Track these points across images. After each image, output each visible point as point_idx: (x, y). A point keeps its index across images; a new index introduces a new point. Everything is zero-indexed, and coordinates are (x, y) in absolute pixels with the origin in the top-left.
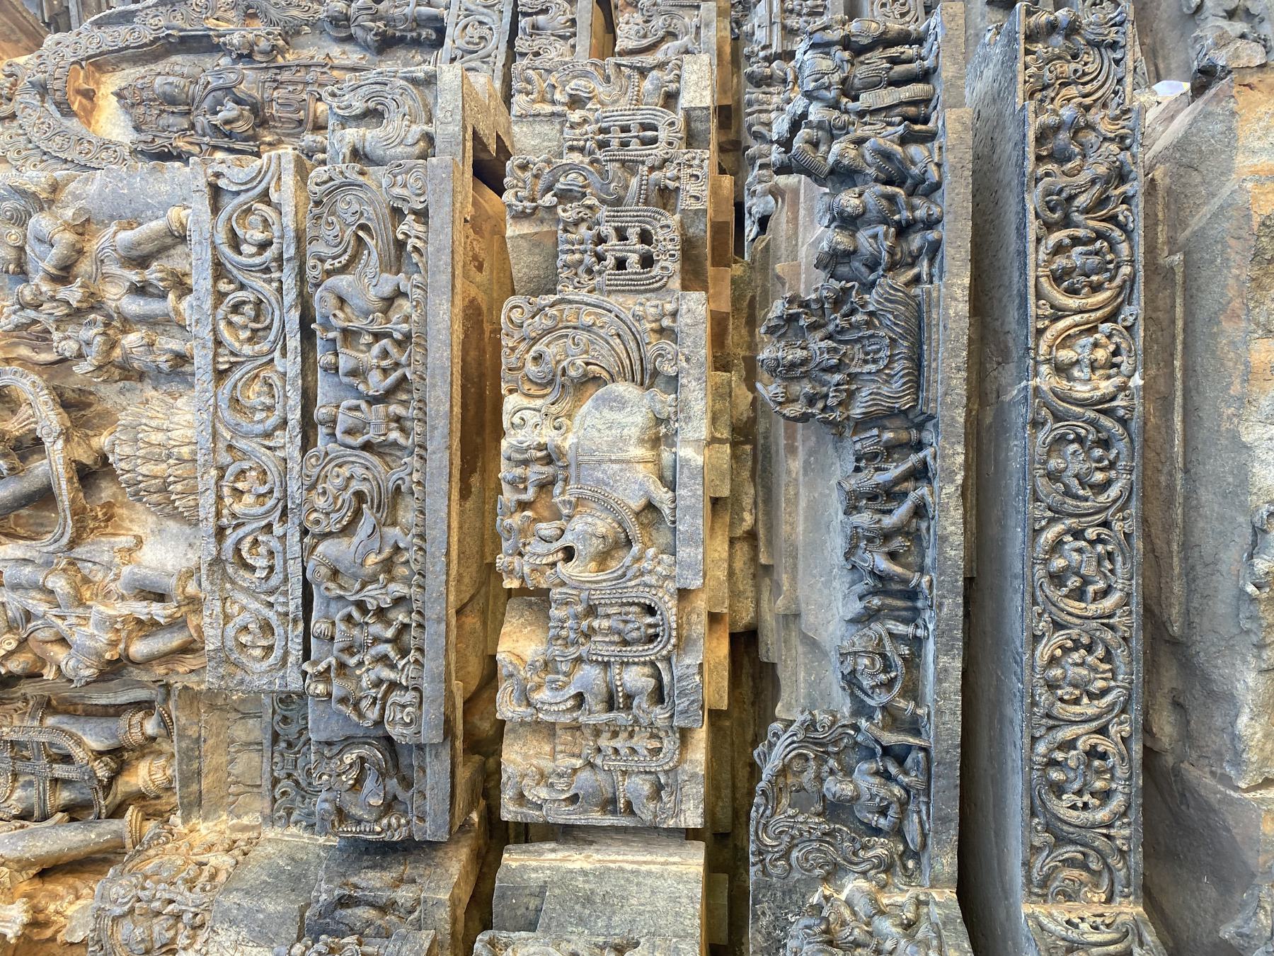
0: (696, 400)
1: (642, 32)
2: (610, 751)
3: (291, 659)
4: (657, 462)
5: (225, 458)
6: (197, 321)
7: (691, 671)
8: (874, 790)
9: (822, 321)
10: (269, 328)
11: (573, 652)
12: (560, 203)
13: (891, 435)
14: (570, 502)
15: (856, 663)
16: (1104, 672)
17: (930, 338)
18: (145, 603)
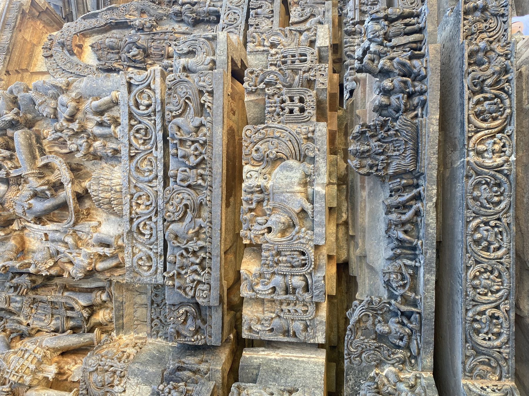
0: (322, 167)
1: (301, 15)
2: (287, 311)
3: (159, 271)
4: (306, 192)
5: (133, 191)
6: (122, 137)
7: (320, 279)
8: (397, 330)
9: (376, 134)
10: (150, 139)
11: (271, 270)
12: (266, 87)
13: (405, 181)
14: (270, 209)
15: (390, 277)
16: (498, 282)
17: (422, 141)
18: (102, 248)
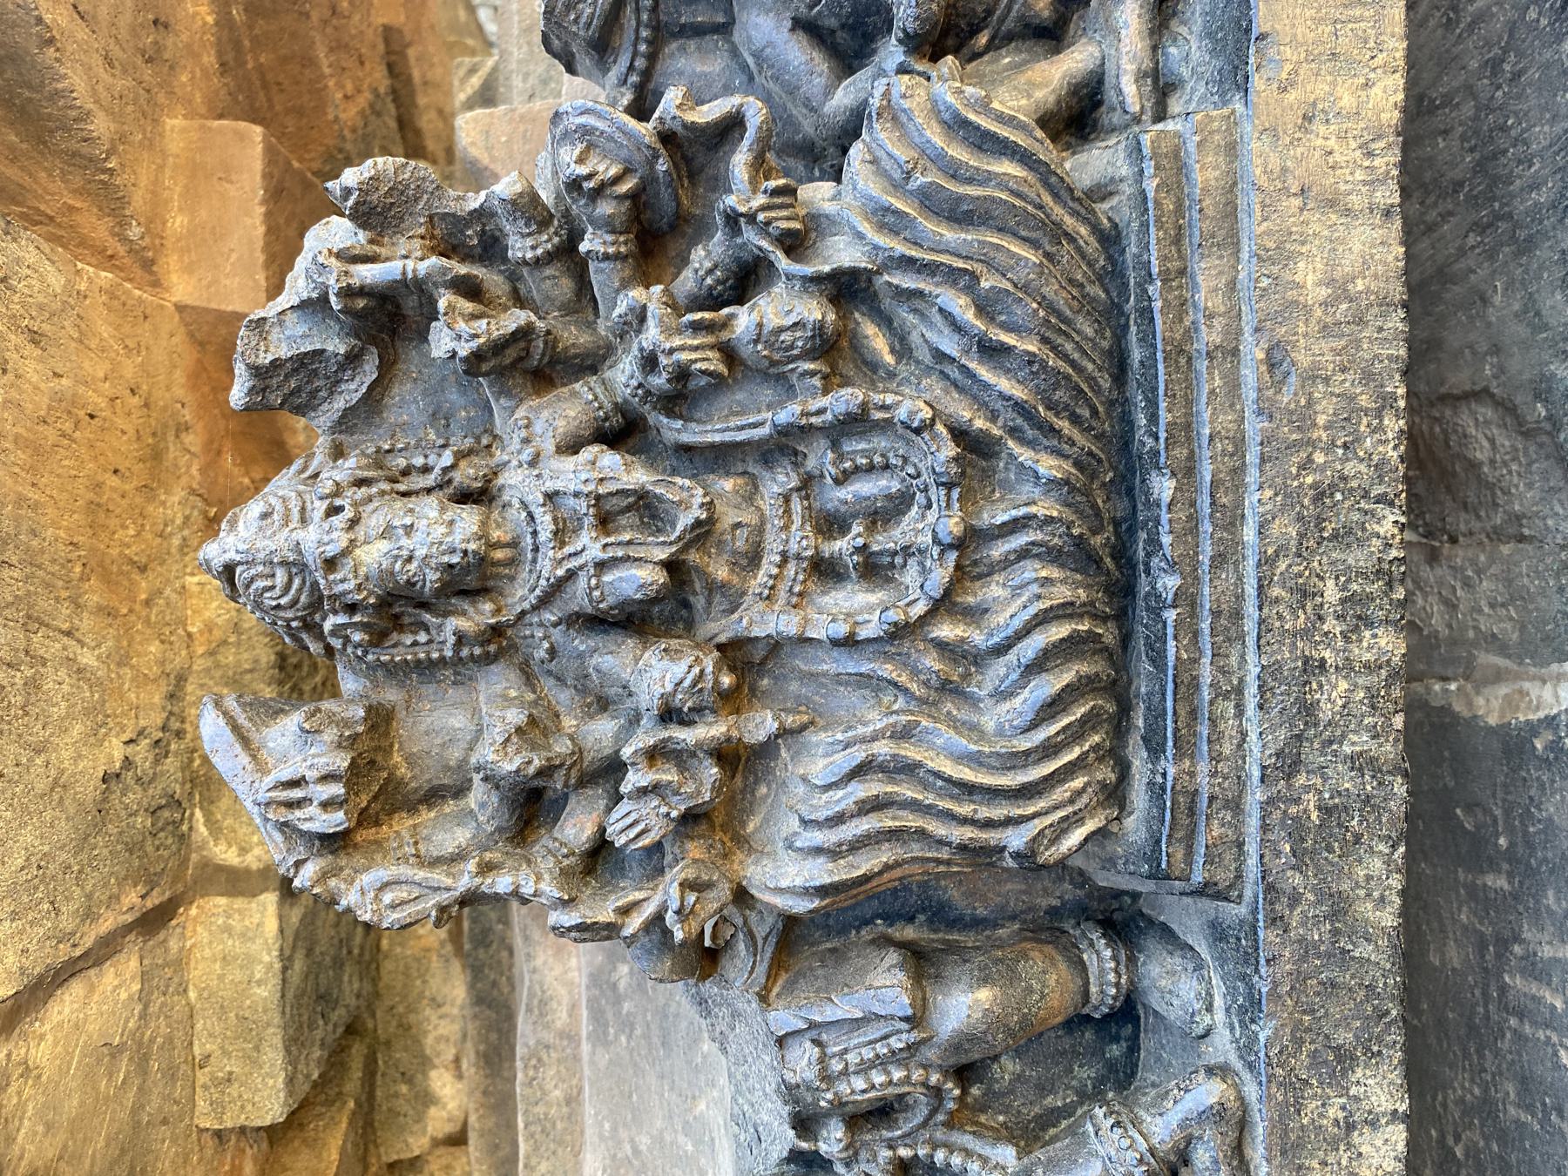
9: (573, 337)
17: (1185, 430)
